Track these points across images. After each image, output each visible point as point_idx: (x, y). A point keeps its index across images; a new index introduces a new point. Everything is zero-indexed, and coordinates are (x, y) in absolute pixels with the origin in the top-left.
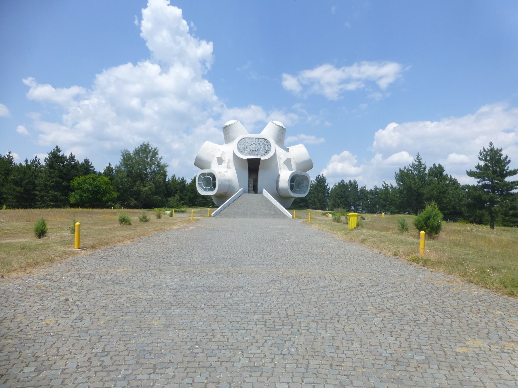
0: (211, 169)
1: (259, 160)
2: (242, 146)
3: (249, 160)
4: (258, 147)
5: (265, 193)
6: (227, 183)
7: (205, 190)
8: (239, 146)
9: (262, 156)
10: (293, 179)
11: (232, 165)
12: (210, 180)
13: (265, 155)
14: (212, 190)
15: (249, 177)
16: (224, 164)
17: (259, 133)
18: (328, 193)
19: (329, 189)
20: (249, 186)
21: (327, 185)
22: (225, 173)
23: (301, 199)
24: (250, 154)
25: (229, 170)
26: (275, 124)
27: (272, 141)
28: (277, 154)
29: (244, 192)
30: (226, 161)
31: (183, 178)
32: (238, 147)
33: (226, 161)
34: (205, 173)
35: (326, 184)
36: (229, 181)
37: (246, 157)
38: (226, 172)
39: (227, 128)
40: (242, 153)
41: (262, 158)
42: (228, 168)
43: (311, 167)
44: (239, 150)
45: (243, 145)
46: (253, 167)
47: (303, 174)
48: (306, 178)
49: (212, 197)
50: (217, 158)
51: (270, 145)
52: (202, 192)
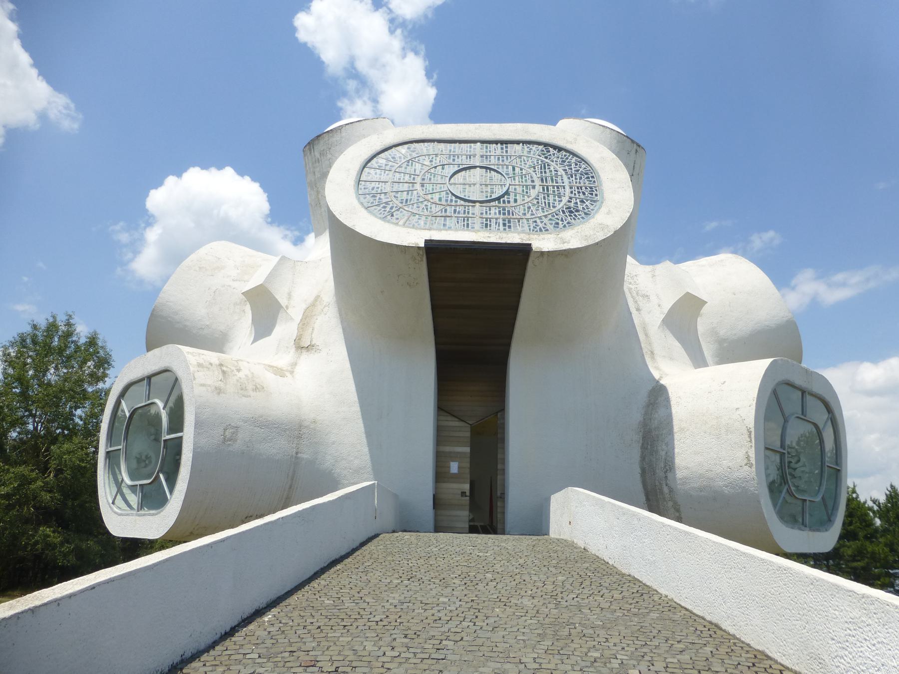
3: (436, 252)
6: (278, 447)
11: (329, 331)
15: (442, 408)
16: (285, 330)
20: (441, 475)
22: (269, 379)
25: (307, 362)
29: (406, 524)
30: (296, 312)
33: (296, 312)
36: (297, 430)
38: (279, 372)
39: (320, 146)
51: (590, 174)
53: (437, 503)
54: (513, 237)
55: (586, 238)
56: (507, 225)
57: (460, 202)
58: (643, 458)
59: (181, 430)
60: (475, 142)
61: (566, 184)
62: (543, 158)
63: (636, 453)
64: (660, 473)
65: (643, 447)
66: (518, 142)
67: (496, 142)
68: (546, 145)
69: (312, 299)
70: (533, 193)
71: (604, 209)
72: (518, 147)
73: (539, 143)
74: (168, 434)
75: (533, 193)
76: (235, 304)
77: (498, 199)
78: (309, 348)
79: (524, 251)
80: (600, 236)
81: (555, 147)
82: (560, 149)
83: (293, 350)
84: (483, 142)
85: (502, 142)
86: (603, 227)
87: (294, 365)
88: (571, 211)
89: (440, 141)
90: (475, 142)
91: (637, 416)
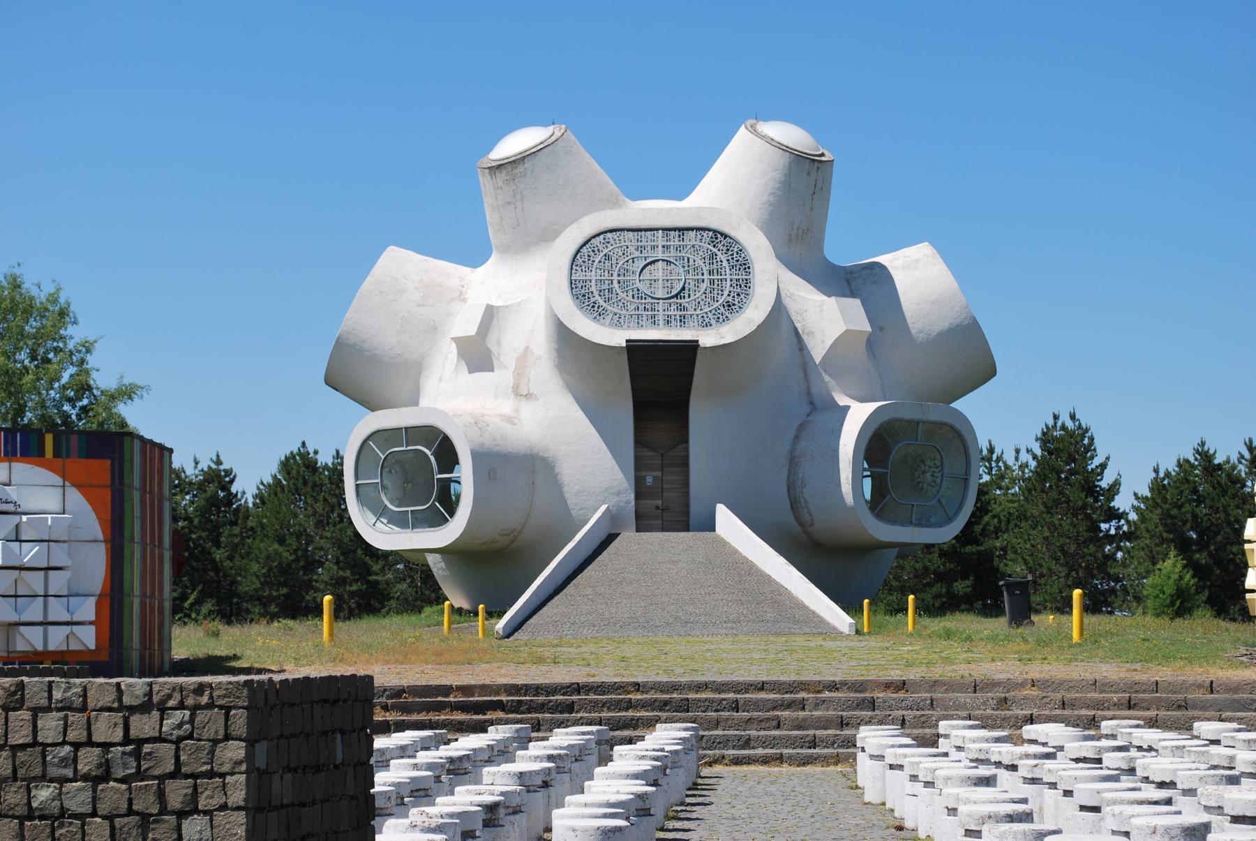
0: (424, 402)
1: (690, 349)
2: (593, 275)
3: (635, 350)
4: (679, 276)
5: (730, 526)
7: (401, 521)
9: (708, 325)
10: (877, 444)
12: (422, 466)
13: (721, 319)
14: (437, 520)
15: (639, 442)
16: (502, 376)
17: (682, 192)
18: (1114, 515)
19: (1114, 489)
21: (1103, 466)
23: (928, 547)
24: (640, 326)
26: (770, 141)
28: (792, 307)
32: (572, 284)
35: (1097, 461)
37: (617, 338)
38: (510, 420)
40: (596, 312)
41: (708, 339)
42: (521, 393)
43: (982, 370)
44: (580, 293)
46: (656, 390)
47: (935, 413)
48: (956, 437)
49: (432, 559)
50: (459, 341)
51: (746, 266)
52: (381, 535)
53: (639, 516)
56: (683, 321)
57: (649, 300)
58: (789, 477)
60: (657, 230)
61: (728, 277)
62: (711, 247)
63: (785, 474)
65: (789, 471)
66: (692, 229)
67: (674, 229)
68: (714, 231)
70: (703, 286)
71: (753, 304)
72: (692, 234)
73: (709, 230)
74: (440, 473)
75: (703, 286)
77: (676, 296)
78: (528, 396)
80: (748, 331)
81: (722, 234)
82: (725, 236)
84: (664, 229)
85: (680, 229)
87: (517, 411)
88: (729, 306)
89: (628, 230)
90: (657, 230)
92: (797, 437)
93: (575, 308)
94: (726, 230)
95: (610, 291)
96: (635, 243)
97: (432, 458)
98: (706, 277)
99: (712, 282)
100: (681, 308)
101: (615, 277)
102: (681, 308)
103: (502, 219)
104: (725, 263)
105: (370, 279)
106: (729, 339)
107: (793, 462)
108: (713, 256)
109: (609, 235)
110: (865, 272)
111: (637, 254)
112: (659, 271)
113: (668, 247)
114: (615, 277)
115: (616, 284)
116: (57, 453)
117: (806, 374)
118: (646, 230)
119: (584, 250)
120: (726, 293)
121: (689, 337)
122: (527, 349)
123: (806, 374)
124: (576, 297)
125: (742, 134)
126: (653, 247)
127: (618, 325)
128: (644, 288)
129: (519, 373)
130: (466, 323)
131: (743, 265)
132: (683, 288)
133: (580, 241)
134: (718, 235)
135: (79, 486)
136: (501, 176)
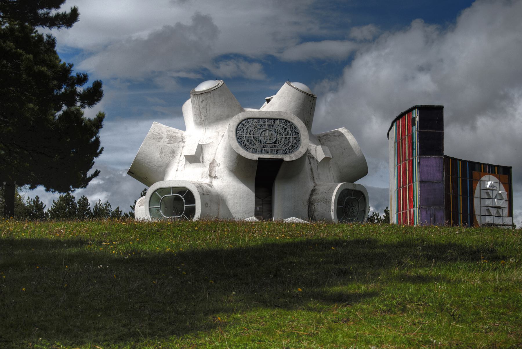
1: (281, 161)
8: (239, 134)
9: (285, 153)
24: (262, 153)
27: (299, 123)
31: (37, 198)
32: (237, 138)
34: (169, 188)
37: (255, 157)
40: (246, 147)
41: (287, 158)
44: (240, 141)
45: (245, 133)
54: (279, 157)
55: (296, 156)
56: (277, 152)
59: (194, 203)
64: (312, 213)
66: (278, 119)
67: (271, 119)
68: (286, 120)
69: (211, 160)
70: (283, 140)
71: (301, 146)
72: (278, 121)
75: (283, 140)
76: (170, 153)
77: (274, 143)
78: (215, 177)
79: (282, 160)
80: (300, 156)
82: (289, 122)
83: (209, 177)
84: (268, 119)
86: (301, 153)
87: (211, 182)
88: (293, 147)
91: (308, 197)
92: (311, 195)
93: (239, 146)
94: (290, 120)
95: (251, 140)
96: (258, 123)
97: (183, 199)
98: (284, 136)
99: (286, 138)
100: (276, 147)
101: (252, 135)
102: (276, 147)
103: (200, 113)
104: (290, 132)
105: (149, 133)
106: (294, 158)
107: (310, 203)
108: (286, 129)
109: (248, 120)
110: (325, 137)
111: (259, 127)
112: (267, 133)
113: (270, 125)
114: (252, 135)
115: (252, 138)
116: (498, 173)
117: (312, 172)
118: (261, 119)
119: (240, 125)
120: (291, 142)
121: (280, 158)
122: (214, 160)
123: (312, 172)
124: (239, 142)
125: (285, 86)
126: (264, 125)
127: (254, 152)
128: (262, 140)
129: (211, 169)
130: (190, 149)
131: (296, 132)
132: (276, 140)
133: (239, 122)
134: (287, 122)
135: (503, 183)
136: (201, 98)
